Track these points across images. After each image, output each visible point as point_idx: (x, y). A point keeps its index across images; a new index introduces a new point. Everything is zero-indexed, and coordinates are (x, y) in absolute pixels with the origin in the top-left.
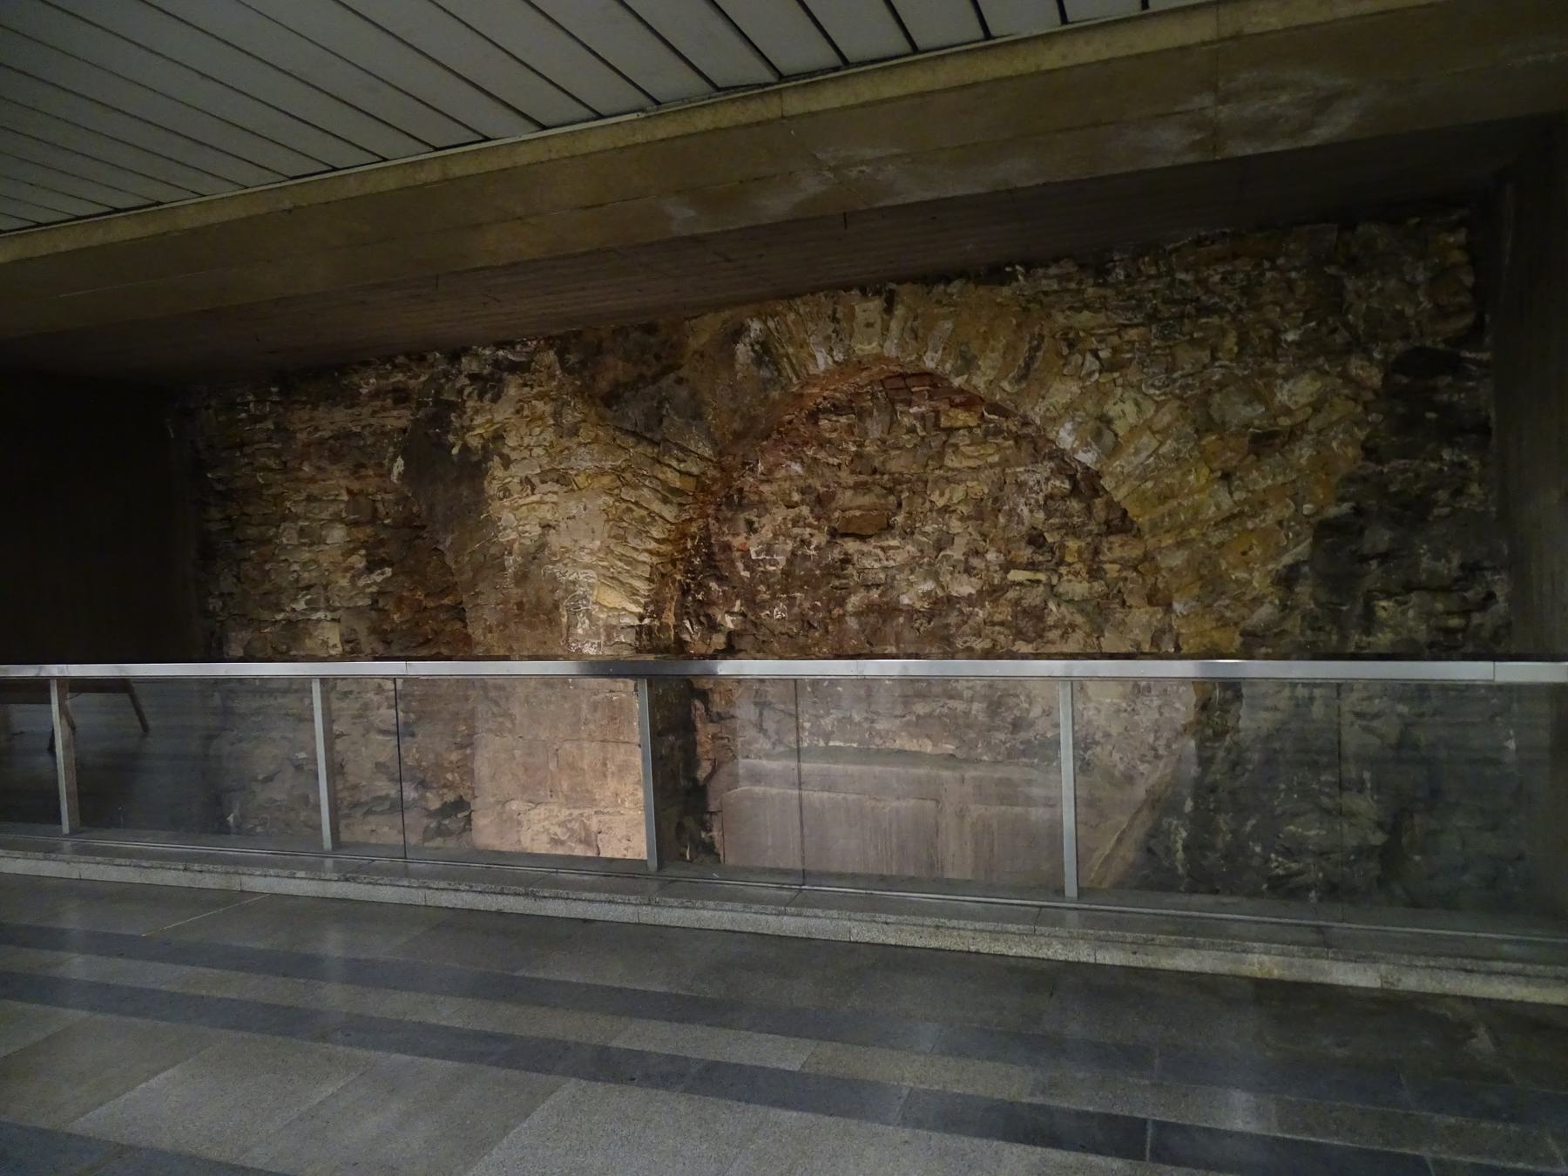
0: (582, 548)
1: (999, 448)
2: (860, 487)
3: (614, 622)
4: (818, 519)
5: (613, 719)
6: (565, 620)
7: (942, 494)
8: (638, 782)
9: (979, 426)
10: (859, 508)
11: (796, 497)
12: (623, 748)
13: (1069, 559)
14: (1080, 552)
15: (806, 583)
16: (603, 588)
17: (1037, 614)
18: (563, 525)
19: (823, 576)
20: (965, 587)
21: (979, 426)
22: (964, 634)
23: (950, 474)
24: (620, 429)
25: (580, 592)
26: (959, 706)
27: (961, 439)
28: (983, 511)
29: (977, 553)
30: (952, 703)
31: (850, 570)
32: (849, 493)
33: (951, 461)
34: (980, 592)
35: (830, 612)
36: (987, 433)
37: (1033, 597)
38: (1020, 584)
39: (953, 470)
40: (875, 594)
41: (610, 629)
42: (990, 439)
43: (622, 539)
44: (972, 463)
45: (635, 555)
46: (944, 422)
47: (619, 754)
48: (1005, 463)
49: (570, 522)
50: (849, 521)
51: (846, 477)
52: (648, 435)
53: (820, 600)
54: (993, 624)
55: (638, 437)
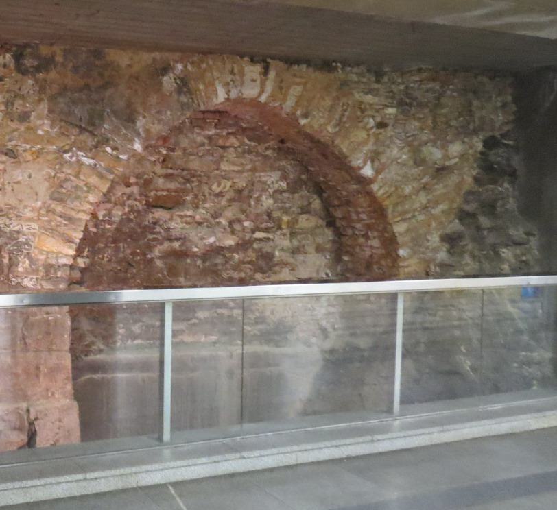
0: (26, 207)
1: (251, 161)
2: (167, 176)
3: (53, 262)
4: (141, 195)
5: (48, 333)
6: (6, 261)
7: (219, 185)
8: (67, 378)
9: (239, 147)
10: (168, 190)
11: (132, 180)
12: (54, 355)
13: (284, 226)
14: (288, 223)
15: (131, 237)
16: (43, 237)
17: (268, 257)
18: (8, 188)
19: (142, 232)
20: (230, 241)
21: (239, 147)
22: (226, 269)
23: (223, 173)
24: (66, 122)
25: (22, 239)
26: (225, 311)
27: (231, 154)
28: (240, 196)
29: (240, 221)
30: (220, 311)
31: (158, 229)
32: (161, 181)
33: (225, 166)
34: (237, 244)
35: (145, 255)
36: (244, 152)
37: (267, 248)
38: (260, 240)
39: (225, 171)
40: (176, 245)
41: (48, 268)
42: (246, 155)
43: (61, 200)
44: (236, 168)
45: (73, 213)
46: (220, 142)
47: (53, 360)
48: (254, 170)
49: (16, 186)
50: (158, 198)
51: (158, 169)
52: (90, 129)
53: (140, 248)
54: (244, 263)
55: (82, 130)
